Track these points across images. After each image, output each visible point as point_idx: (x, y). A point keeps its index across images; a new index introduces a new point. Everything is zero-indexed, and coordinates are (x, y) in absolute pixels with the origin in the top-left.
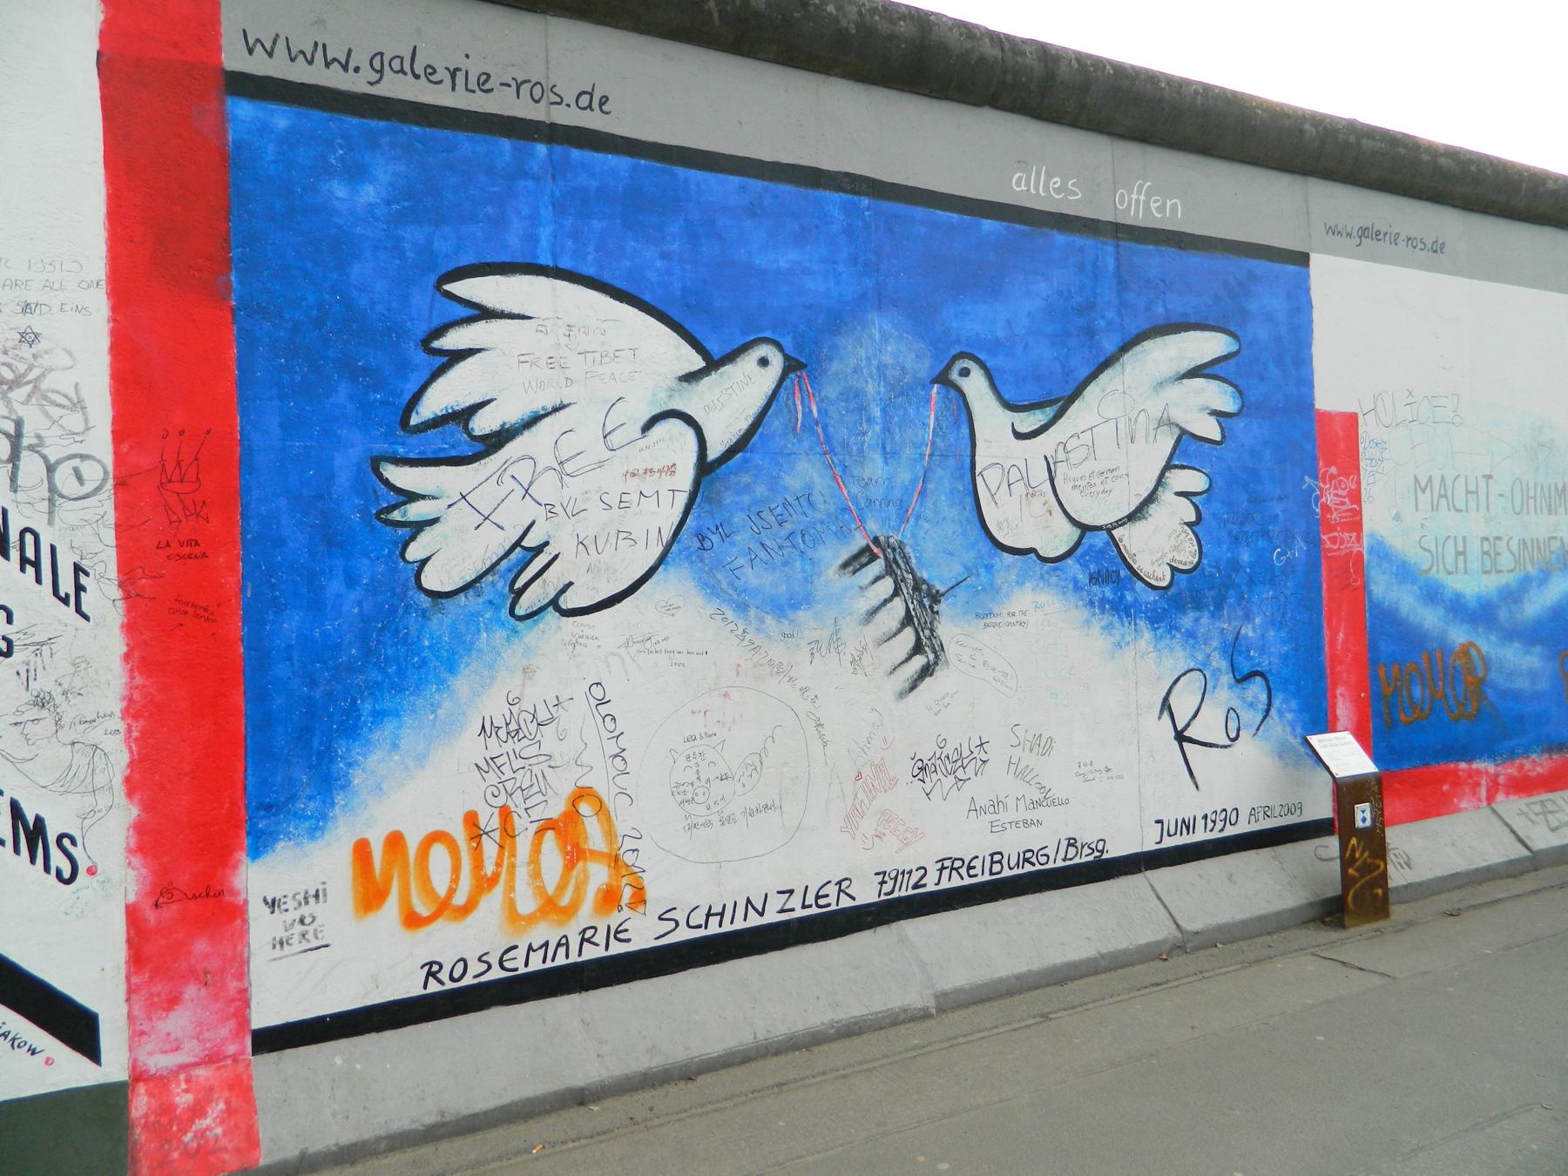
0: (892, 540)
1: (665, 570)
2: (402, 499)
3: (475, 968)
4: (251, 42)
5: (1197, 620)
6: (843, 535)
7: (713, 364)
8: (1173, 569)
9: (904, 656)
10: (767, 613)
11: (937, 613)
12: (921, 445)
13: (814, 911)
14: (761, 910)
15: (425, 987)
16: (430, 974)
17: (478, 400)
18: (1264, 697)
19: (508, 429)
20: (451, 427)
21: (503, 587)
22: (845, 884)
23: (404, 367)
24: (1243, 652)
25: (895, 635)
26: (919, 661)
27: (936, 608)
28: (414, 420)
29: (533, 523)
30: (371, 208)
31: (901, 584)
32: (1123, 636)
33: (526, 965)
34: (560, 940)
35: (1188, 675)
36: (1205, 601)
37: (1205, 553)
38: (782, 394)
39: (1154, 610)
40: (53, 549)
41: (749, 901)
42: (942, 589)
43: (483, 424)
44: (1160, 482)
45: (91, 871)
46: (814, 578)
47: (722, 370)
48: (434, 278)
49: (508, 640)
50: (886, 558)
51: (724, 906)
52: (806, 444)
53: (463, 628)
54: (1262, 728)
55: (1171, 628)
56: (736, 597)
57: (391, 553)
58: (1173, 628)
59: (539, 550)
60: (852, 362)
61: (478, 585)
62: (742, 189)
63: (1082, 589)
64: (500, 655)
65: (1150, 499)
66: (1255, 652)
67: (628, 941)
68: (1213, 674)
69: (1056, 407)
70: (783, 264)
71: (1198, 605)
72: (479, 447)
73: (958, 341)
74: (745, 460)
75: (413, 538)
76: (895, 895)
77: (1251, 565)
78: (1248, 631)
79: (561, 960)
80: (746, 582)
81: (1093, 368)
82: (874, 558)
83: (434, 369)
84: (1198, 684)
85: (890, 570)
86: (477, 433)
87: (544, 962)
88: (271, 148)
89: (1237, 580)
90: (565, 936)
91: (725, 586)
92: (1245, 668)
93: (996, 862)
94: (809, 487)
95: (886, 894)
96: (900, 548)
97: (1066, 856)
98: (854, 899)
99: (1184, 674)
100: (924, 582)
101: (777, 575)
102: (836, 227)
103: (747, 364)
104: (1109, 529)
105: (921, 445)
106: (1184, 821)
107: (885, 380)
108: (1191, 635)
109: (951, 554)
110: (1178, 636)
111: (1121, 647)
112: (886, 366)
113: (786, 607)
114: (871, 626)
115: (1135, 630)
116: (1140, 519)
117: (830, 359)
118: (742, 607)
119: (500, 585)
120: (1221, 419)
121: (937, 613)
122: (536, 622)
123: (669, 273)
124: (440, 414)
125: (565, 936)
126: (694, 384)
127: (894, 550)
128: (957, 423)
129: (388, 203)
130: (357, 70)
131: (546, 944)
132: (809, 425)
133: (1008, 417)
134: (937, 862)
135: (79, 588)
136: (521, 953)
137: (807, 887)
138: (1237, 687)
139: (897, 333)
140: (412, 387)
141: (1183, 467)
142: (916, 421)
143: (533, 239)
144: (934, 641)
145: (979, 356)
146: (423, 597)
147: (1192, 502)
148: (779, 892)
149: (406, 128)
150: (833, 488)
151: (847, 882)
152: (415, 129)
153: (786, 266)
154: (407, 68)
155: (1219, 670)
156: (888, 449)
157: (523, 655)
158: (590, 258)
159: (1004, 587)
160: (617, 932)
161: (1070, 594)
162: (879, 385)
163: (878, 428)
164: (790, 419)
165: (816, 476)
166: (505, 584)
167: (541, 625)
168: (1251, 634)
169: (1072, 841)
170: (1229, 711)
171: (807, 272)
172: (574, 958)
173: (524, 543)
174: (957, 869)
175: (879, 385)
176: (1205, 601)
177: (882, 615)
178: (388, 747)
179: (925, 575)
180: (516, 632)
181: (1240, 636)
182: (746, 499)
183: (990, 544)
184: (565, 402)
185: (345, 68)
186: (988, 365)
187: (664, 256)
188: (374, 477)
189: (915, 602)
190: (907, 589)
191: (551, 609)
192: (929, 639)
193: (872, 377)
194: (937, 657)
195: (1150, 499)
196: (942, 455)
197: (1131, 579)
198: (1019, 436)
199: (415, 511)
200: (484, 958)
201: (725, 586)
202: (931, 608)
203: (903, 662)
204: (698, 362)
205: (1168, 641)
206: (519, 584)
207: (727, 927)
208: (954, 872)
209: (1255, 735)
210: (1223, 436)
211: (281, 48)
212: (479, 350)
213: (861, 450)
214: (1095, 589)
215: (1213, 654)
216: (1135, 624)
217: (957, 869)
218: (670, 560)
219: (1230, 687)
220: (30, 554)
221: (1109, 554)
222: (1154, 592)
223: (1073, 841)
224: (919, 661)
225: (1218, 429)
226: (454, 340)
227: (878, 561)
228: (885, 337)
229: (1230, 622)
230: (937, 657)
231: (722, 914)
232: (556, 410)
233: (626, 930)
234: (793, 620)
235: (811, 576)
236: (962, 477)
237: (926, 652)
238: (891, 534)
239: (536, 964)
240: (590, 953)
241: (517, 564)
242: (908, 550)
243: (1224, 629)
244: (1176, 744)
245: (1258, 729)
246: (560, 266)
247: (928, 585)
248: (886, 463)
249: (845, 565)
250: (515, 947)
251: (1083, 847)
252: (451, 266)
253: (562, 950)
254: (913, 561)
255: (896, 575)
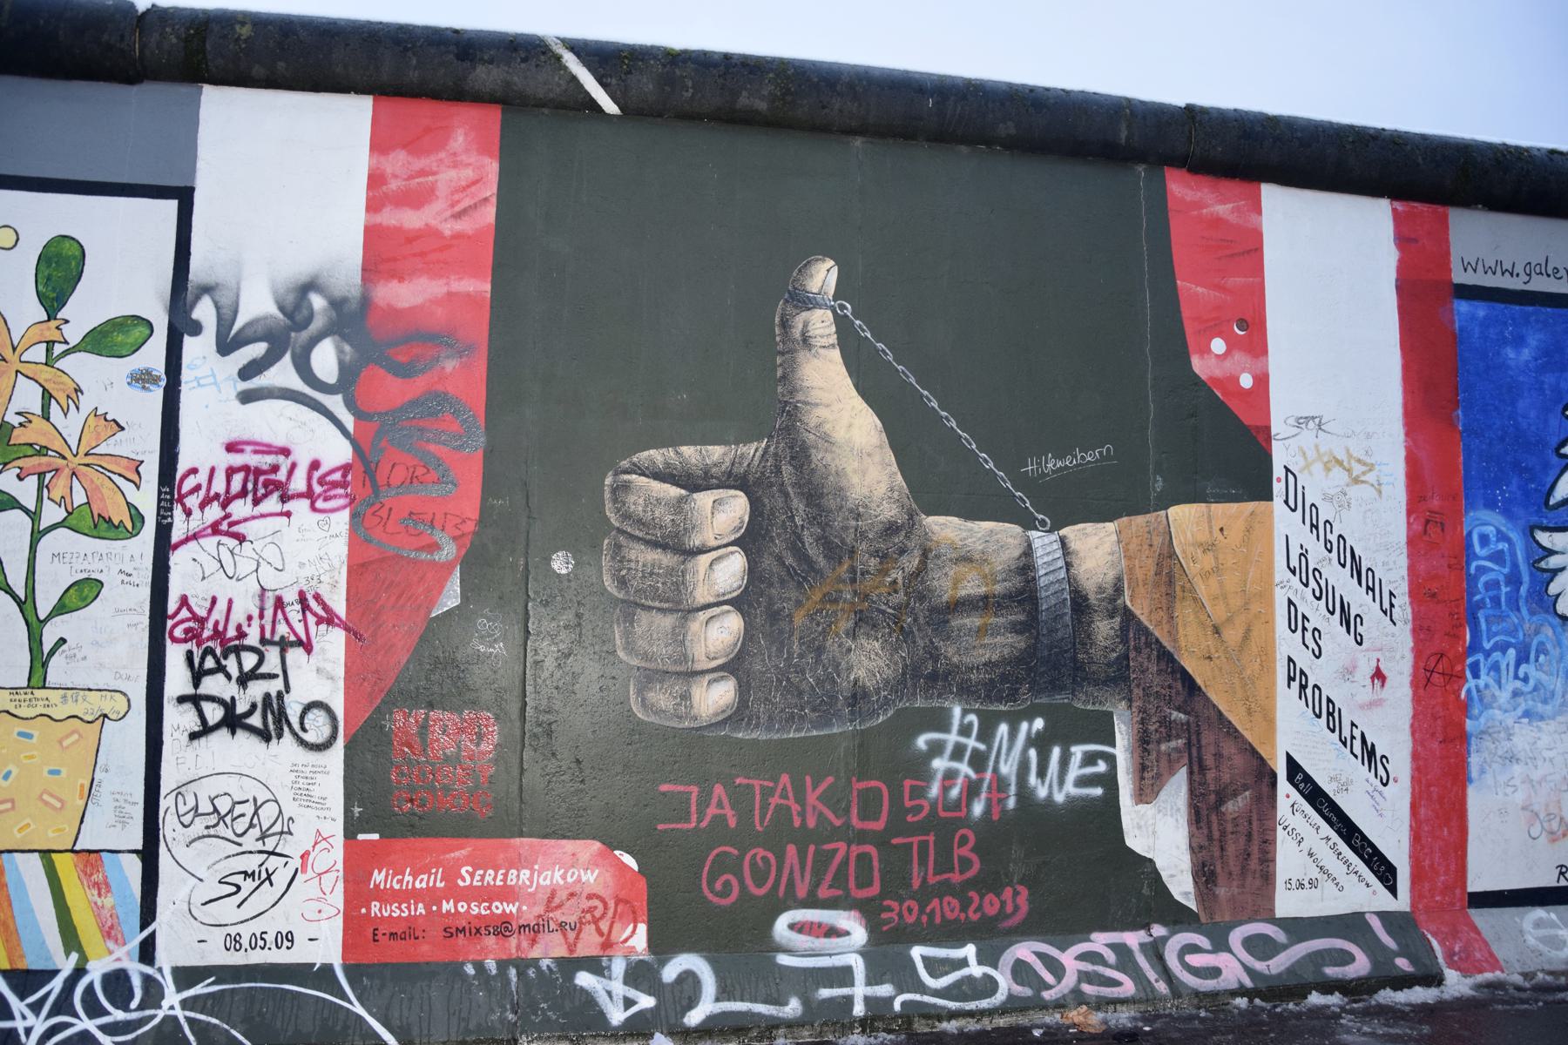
4: (1466, 264)
15: (1558, 881)
23: (1546, 466)
30: (1527, 362)
40: (1380, 580)
45: (1396, 781)
48: (1561, 407)
57: (1541, 588)
75: (1552, 580)
88: (1477, 330)
130: (1518, 275)
135: (1392, 605)
140: (1550, 480)
149: (1543, 309)
154: (1543, 271)
185: (1512, 275)
199: (1553, 562)
211: (1480, 267)
220: (1371, 584)
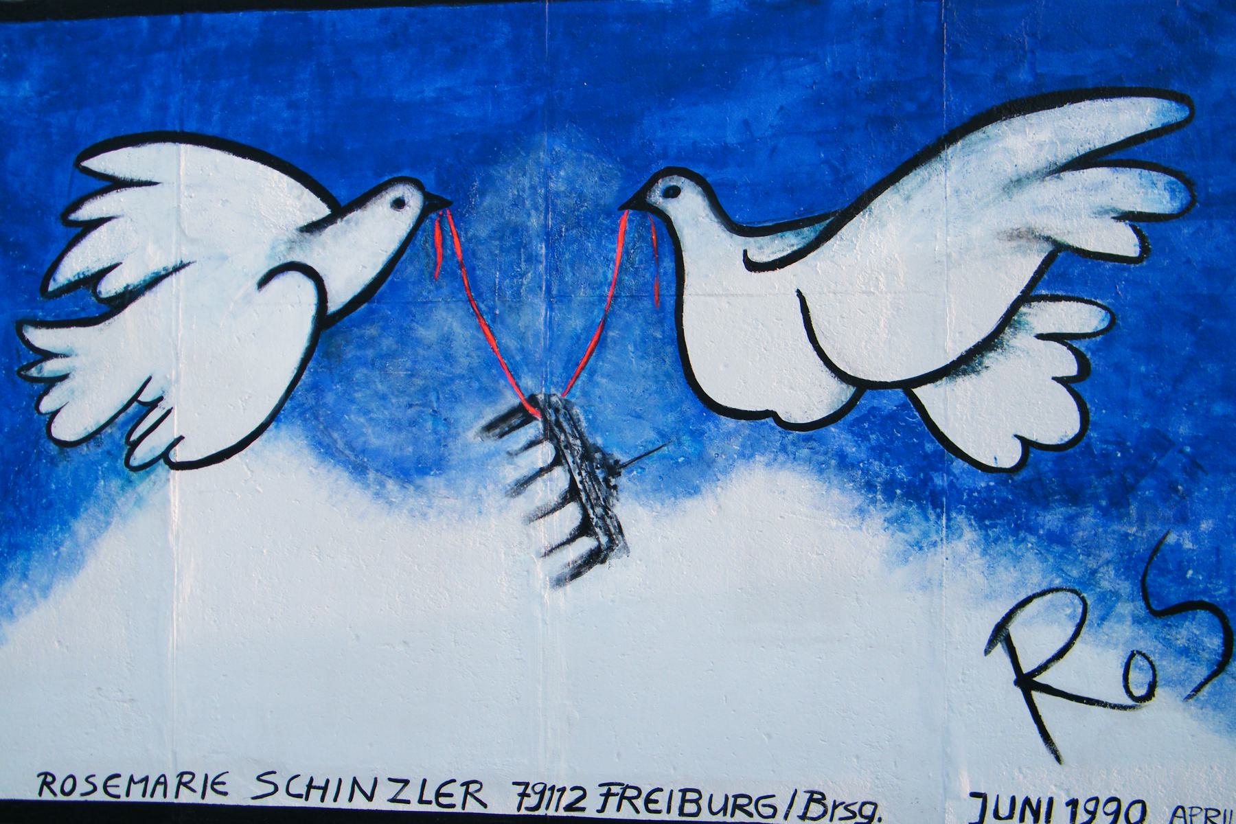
0: (554, 399)
1: (276, 427)
2: (39, 357)
3: (83, 787)
5: (1071, 519)
6: (488, 394)
7: (339, 211)
8: (1027, 445)
9: (565, 536)
10: (390, 477)
11: (615, 487)
12: (601, 284)
13: (434, 808)
14: (369, 795)
15: (40, 794)
16: (45, 783)
17: (106, 265)
18: (1214, 643)
19: (131, 291)
20: (82, 290)
21: (120, 439)
22: (473, 788)
24: (1170, 572)
25: (554, 510)
26: (585, 544)
27: (613, 482)
28: (52, 287)
29: (149, 379)
31: (565, 451)
32: (926, 534)
33: (128, 794)
34: (159, 778)
35: (1049, 596)
36: (1089, 491)
37: (1095, 424)
38: (419, 237)
39: (989, 500)
41: (355, 782)
42: (624, 459)
43: (110, 287)
44: (1009, 319)
46: (448, 440)
47: (349, 216)
48: (74, 157)
49: (123, 488)
50: (545, 421)
51: (328, 781)
52: (445, 291)
53: (83, 474)
54: (1207, 688)
55: (1018, 528)
56: (352, 458)
57: (28, 405)
58: (1021, 528)
59: (153, 405)
60: (512, 193)
61: (98, 436)
62: (384, 20)
63: (853, 466)
64: (114, 502)
65: (990, 343)
66: (1196, 572)
67: (225, 794)
68: (1102, 598)
69: (820, 227)
70: (429, 93)
71: (1075, 496)
72: (105, 308)
73: (665, 156)
74: (371, 311)
75: (46, 392)
76: (541, 812)
77: (1195, 442)
78: (1181, 539)
79: (159, 798)
80: (365, 442)
81: (891, 169)
82: (528, 419)
83: (70, 239)
84: (1069, 611)
85: (550, 434)
86: (104, 295)
87: (144, 795)
89: (1161, 463)
90: (164, 776)
91: (340, 445)
92: (1175, 595)
93: (691, 801)
94: (447, 339)
95: (527, 809)
96: (565, 407)
97: (805, 813)
98: (485, 806)
99: (1043, 593)
100: (598, 449)
101: (403, 435)
102: (499, 42)
103: (381, 207)
104: (908, 385)
105: (601, 284)
106: (1027, 801)
107: (554, 212)
108: (1058, 539)
109: (639, 417)
110: (1033, 539)
111: (921, 548)
112: (557, 194)
113: (412, 472)
114: (521, 499)
115: (948, 527)
116: (965, 373)
117: (483, 193)
118: (359, 470)
119: (118, 435)
120: (1140, 225)
121: (615, 487)
122: (148, 474)
123: (296, 121)
124: (73, 280)
125: (164, 776)
126: (317, 234)
127: (557, 411)
128: (657, 258)
129: (40, 94)
131: (146, 779)
132: (451, 268)
133: (735, 245)
134: (601, 785)
136: (123, 782)
137: (425, 781)
138: (1153, 622)
139: (574, 154)
140: (51, 257)
141: (1055, 299)
142: (596, 256)
143: (163, 108)
144: (608, 521)
145: (696, 170)
146: (52, 446)
147: (1071, 348)
148: (390, 780)
149: (58, 24)
150: (479, 339)
151: (477, 786)
152: (66, 23)
153: (432, 94)
155: (1116, 594)
156: (554, 292)
157: (135, 503)
158: (215, 118)
159: (721, 460)
160: (214, 783)
161: (831, 473)
162: (546, 218)
163: (541, 268)
164: (428, 264)
165: (457, 328)
166: (122, 436)
167: (153, 477)
168: (1188, 545)
169: (816, 796)
170: (1132, 656)
171: (460, 98)
172: (171, 798)
173: (141, 398)
174: (630, 799)
175: (546, 218)
176: (1089, 491)
177: (538, 485)
178: (19, 576)
179: (599, 441)
180: (130, 482)
181: (1162, 547)
182: (370, 353)
183: (700, 405)
184: (185, 261)
186: (709, 180)
187: (292, 105)
188: (18, 338)
189: (584, 473)
190: (574, 457)
191: (162, 461)
192: (602, 518)
193: (537, 209)
194: (611, 541)
195: (990, 343)
196: (632, 296)
197: (942, 455)
198: (752, 266)
199: (50, 368)
200: (90, 780)
201: (340, 445)
202: (607, 481)
203: (563, 544)
204: (323, 210)
205: (1011, 547)
206: (134, 437)
207: (329, 803)
208: (625, 802)
209: (1189, 697)
210: (1144, 249)
212: (109, 219)
213: (517, 294)
214: (876, 465)
215: (1102, 570)
216: (949, 519)
217: (630, 799)
218: (282, 417)
219: (1137, 621)
221: (905, 421)
222: (987, 476)
223: (820, 797)
224: (585, 544)
225: (1134, 239)
226: (88, 211)
227: (534, 423)
228: (557, 162)
229: (1141, 521)
230: (611, 541)
231: (325, 789)
232: (177, 269)
233: (223, 783)
234: (419, 487)
235: (445, 438)
236: (661, 322)
237: (596, 534)
238: (553, 391)
239: (136, 796)
240: (186, 797)
241: (132, 419)
242: (577, 411)
243: (1127, 535)
244: (1018, 693)
245: (1197, 690)
246: (186, 130)
247: (603, 454)
248: (550, 307)
249: (489, 427)
250: (118, 776)
251: (835, 807)
252: (89, 144)
253: (160, 789)
254: (584, 424)
255: (558, 440)
